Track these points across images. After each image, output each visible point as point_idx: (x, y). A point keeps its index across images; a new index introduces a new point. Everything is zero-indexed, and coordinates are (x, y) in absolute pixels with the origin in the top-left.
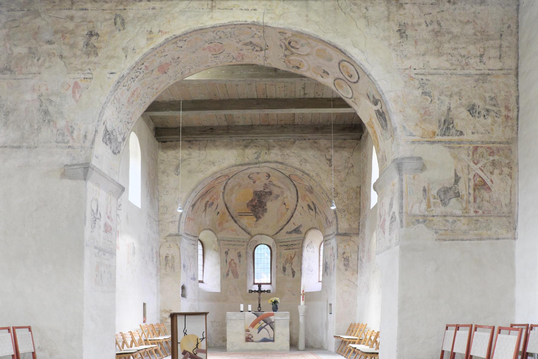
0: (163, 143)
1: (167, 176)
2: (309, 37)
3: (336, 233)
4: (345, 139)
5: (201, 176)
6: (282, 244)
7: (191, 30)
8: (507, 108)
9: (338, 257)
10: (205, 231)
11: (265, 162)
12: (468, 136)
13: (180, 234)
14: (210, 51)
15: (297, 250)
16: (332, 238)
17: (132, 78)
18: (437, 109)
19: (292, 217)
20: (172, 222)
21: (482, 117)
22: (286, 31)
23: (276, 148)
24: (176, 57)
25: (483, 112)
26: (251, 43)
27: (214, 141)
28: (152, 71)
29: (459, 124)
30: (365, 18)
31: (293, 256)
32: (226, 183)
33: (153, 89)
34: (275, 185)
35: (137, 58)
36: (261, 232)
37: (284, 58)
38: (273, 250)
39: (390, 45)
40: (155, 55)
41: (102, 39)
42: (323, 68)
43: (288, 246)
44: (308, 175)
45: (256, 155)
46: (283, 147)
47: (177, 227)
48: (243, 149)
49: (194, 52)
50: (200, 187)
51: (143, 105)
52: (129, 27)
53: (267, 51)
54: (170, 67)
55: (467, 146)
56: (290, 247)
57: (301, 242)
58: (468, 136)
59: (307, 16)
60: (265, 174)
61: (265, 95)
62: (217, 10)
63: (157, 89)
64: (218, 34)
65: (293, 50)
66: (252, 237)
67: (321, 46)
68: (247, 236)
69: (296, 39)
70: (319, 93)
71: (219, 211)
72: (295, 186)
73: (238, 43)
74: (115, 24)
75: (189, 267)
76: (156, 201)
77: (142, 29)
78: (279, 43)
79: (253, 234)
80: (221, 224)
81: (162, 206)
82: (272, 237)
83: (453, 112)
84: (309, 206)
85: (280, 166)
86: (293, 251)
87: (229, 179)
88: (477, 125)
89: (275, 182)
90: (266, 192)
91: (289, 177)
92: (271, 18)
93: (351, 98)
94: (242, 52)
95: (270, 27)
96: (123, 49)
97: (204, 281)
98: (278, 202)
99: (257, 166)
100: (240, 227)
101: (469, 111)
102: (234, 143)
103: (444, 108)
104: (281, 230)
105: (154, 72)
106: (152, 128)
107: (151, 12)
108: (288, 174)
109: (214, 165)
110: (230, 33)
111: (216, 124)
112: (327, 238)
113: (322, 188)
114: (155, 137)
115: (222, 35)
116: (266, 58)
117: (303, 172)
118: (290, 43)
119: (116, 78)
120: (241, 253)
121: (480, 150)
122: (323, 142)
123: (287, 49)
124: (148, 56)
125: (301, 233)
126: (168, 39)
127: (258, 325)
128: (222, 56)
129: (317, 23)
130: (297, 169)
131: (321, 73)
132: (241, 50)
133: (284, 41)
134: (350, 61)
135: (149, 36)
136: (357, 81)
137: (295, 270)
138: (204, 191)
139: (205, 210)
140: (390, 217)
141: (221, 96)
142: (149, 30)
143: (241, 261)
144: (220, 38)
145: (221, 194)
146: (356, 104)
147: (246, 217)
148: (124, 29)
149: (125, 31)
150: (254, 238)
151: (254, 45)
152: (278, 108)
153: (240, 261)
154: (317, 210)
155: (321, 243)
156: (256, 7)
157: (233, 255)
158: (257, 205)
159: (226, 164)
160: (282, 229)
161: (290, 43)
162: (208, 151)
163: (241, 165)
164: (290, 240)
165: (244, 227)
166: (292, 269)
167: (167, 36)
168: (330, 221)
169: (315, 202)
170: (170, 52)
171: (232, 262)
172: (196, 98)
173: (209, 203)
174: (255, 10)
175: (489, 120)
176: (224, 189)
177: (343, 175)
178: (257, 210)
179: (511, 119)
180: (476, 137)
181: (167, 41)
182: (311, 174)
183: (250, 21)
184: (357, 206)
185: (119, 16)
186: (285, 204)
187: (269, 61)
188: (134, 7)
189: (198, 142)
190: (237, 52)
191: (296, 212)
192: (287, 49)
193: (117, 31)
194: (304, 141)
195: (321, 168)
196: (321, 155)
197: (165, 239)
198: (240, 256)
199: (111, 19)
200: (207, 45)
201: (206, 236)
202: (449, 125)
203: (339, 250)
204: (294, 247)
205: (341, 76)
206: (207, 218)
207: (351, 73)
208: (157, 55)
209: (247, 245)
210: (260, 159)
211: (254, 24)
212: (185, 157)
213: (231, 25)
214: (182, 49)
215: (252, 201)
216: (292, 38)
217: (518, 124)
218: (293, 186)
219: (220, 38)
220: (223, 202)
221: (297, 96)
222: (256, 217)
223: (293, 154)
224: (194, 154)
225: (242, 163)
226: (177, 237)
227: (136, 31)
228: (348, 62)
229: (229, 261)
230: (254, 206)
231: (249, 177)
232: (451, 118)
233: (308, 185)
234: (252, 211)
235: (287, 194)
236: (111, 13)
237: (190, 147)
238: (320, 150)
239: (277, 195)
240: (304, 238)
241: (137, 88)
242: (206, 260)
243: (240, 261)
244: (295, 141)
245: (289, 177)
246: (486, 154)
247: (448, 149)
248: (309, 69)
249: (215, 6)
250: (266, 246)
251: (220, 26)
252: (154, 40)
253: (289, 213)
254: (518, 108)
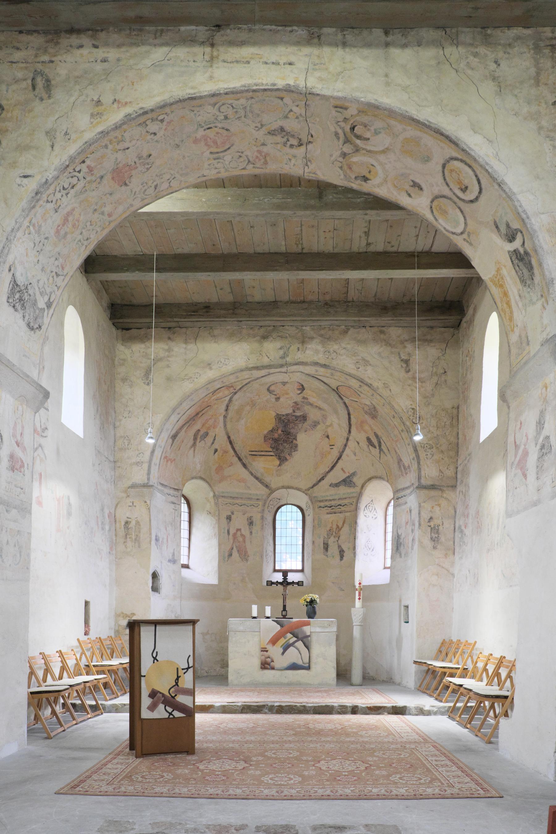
0: (124, 331)
1: (131, 386)
2: (391, 113)
3: (417, 484)
4: (432, 328)
5: (188, 387)
6: (322, 504)
7: (172, 100)
9: (420, 525)
10: (194, 481)
11: (296, 364)
13: (151, 483)
14: (206, 144)
15: (348, 514)
16: (410, 494)
17: (64, 188)
19: (339, 459)
20: (137, 463)
22: (347, 104)
23: (315, 341)
24: (145, 154)
26: (282, 129)
27: (211, 328)
28: (102, 177)
30: (494, 79)
31: (340, 525)
32: (230, 400)
33: (103, 213)
34: (311, 405)
35: (73, 149)
36: (286, 484)
37: (341, 159)
38: (306, 514)
39: (540, 128)
40: (106, 146)
41: (9, 115)
42: (412, 177)
43: (333, 508)
44: (369, 386)
45: (281, 352)
46: (329, 339)
47: (146, 472)
48: (260, 342)
49: (178, 146)
50: (186, 405)
51: (86, 243)
52: (59, 94)
53: (310, 147)
54: (133, 172)
56: (337, 510)
57: (355, 500)
59: (386, 76)
60: (296, 386)
61: (300, 246)
62: (221, 64)
63: (110, 215)
64: (223, 109)
65: (358, 142)
66: (272, 491)
67: (411, 132)
68: (264, 491)
69: (365, 119)
70: (393, 243)
71: (217, 447)
72: (347, 407)
73: (258, 129)
74: (34, 87)
75: (165, 541)
76: (111, 427)
77: (83, 97)
78: (333, 130)
79: (273, 486)
80: (220, 469)
81: (121, 437)
82: (305, 492)
84: (369, 439)
85: (322, 370)
86: (342, 516)
87: (235, 393)
89: (312, 400)
90: (296, 417)
91: (336, 391)
92: (321, 79)
93: (462, 233)
94: (265, 149)
95: (318, 95)
96: (47, 133)
97: (190, 565)
98: (317, 434)
99: (284, 369)
100: (252, 474)
102: (244, 331)
104: (320, 481)
105: (105, 181)
106: (105, 305)
107: (99, 67)
108: (334, 384)
109: (211, 369)
110: (245, 108)
111: (215, 299)
112: (399, 495)
113: (393, 408)
114: (110, 319)
115: (230, 112)
116: (307, 161)
117: (362, 381)
118: (353, 129)
119: (32, 185)
120: (254, 519)
122: (395, 332)
123: (347, 141)
124: (92, 147)
125: (354, 485)
126: (130, 115)
127: (282, 641)
128: (228, 157)
129: (405, 89)
130: (350, 375)
131: (407, 187)
132: (263, 144)
133: (342, 124)
134: (467, 158)
135: (96, 110)
136: (477, 199)
137: (344, 547)
138: (192, 412)
139: (194, 445)
140: (538, 447)
141: (224, 247)
142: (95, 99)
143: (254, 532)
144: (226, 118)
145: (221, 419)
146: (471, 244)
147: (263, 458)
148: (49, 97)
149: (51, 101)
150: (276, 494)
151: (288, 133)
152: (321, 268)
153: (251, 532)
154: (383, 447)
155: (389, 503)
156: (292, 59)
157: (239, 521)
158: (282, 439)
159: (230, 367)
160: (322, 479)
161: (353, 129)
162: (200, 345)
163: (257, 368)
164: (336, 497)
165: (259, 475)
166: (339, 547)
167: (128, 110)
168: (406, 464)
169: (379, 434)
170: (134, 142)
171: (239, 533)
172: (180, 251)
173: (201, 433)
174: (290, 64)
176: (227, 410)
177: (429, 386)
178: (281, 447)
181: (129, 119)
182: (375, 384)
183: (281, 83)
184: (452, 439)
185: (42, 74)
186: (328, 437)
187: (312, 167)
188: (69, 58)
189: (184, 330)
190: (255, 149)
191: (347, 451)
192: (347, 141)
193: (37, 100)
194: (364, 330)
195: (391, 375)
196: (392, 353)
197: (125, 492)
198: (251, 523)
199: (25, 80)
200: (201, 133)
201: (194, 488)
203: (422, 513)
204: (343, 508)
205: (446, 191)
206: (197, 459)
207: (466, 182)
208: (110, 147)
209: (264, 505)
210: (288, 359)
211: (288, 90)
212: (162, 354)
213: (247, 91)
214: (156, 138)
215: (272, 431)
216: (358, 118)
218: (342, 405)
219: (226, 118)
220: (224, 432)
221: (355, 249)
222: (279, 458)
223: (344, 351)
224: (176, 349)
225: (259, 365)
226: (145, 490)
227: (72, 100)
228: (462, 161)
229: (232, 531)
230: (276, 440)
231: (268, 390)
233: (368, 403)
234: (273, 448)
235: (332, 419)
236: (26, 68)
237: (169, 338)
238: (390, 345)
239: (315, 422)
240: (360, 495)
241: (73, 210)
242: (194, 530)
243: (251, 532)
244: (348, 329)
245: (336, 391)
248: (385, 181)
249: (217, 57)
250: (295, 508)
251: (226, 94)
252: (104, 117)
253: (335, 453)
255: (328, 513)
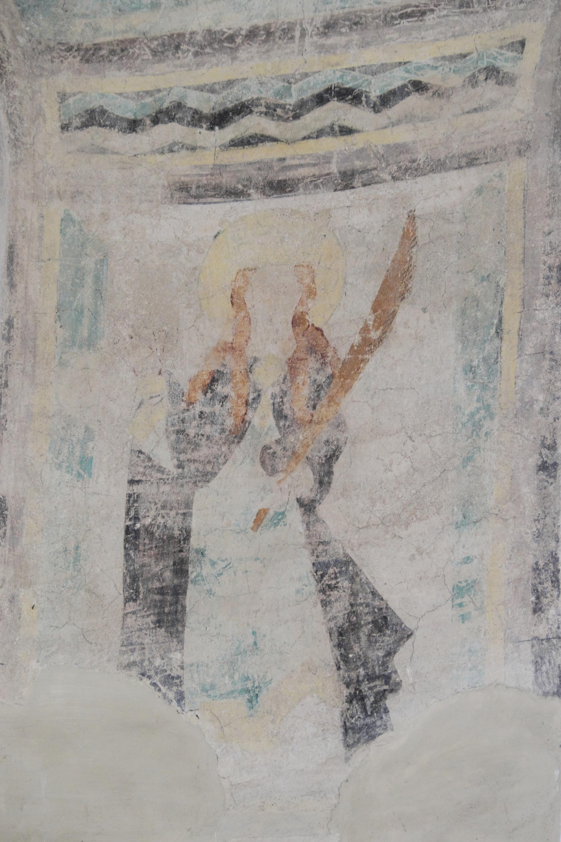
6: (116, 88)
31: (343, 317)
56: (297, 148)
137: (396, 577)
166: (332, 571)
255: (187, 192)
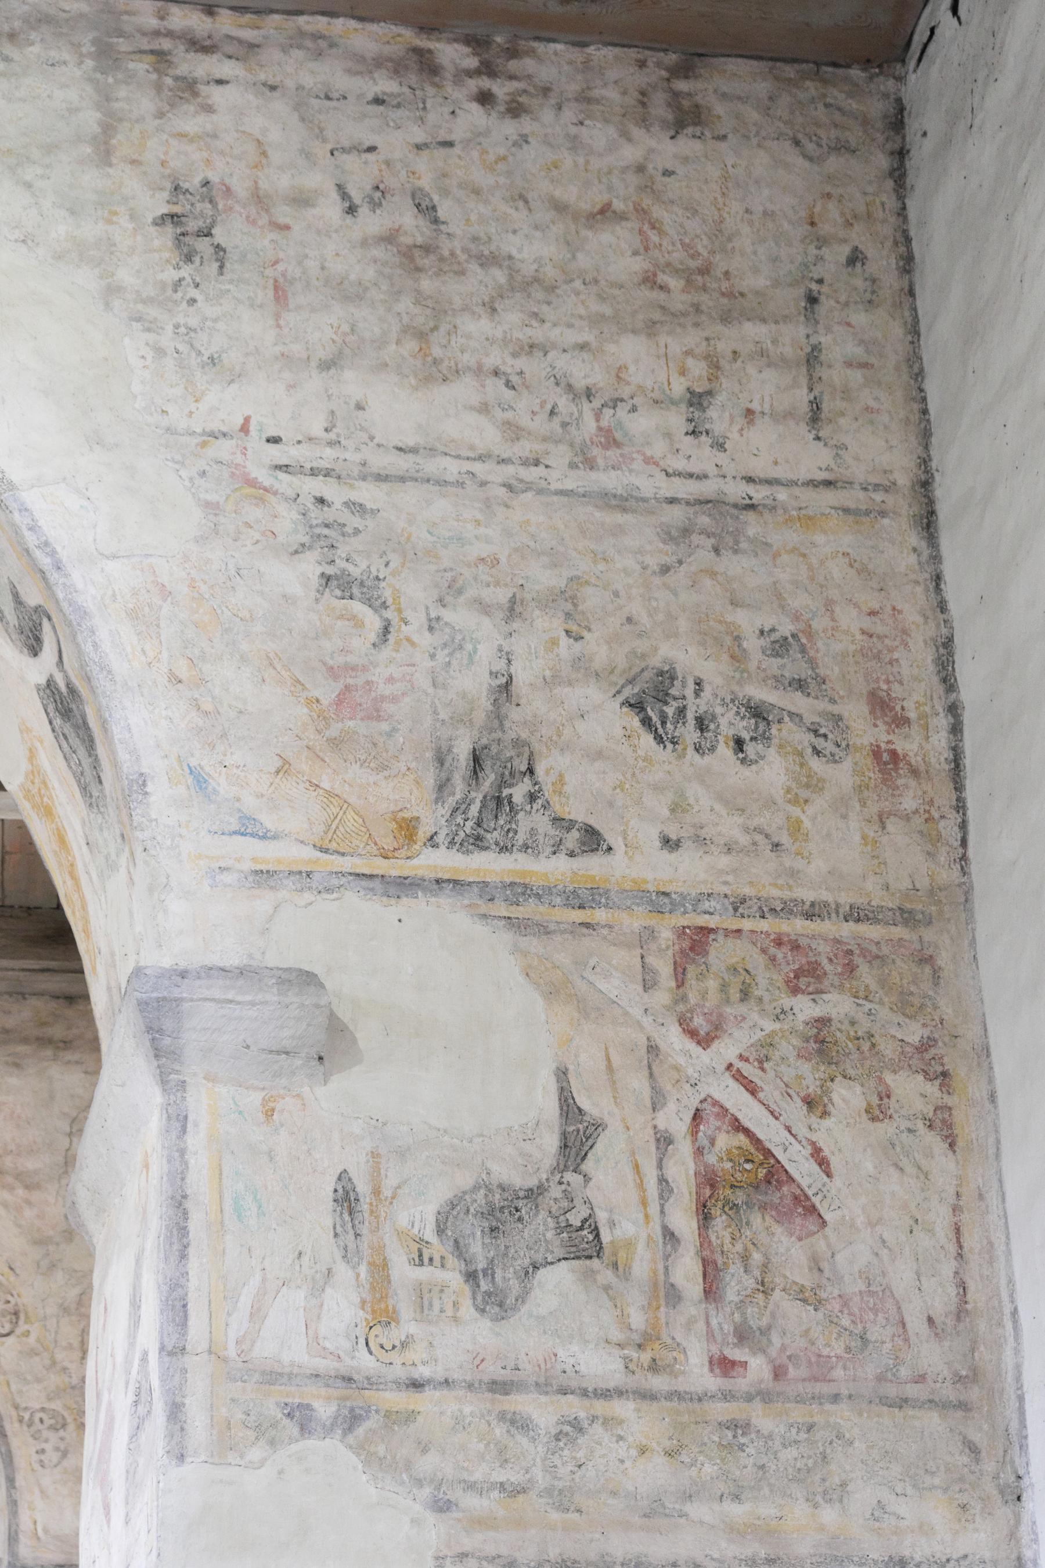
8: (881, 705)
12: (635, 861)
18: (423, 681)
21: (725, 751)
25: (731, 723)
29: (576, 783)
55: (634, 921)
58: (635, 861)
83: (532, 704)
88: (695, 791)
101: (637, 706)
103: (473, 682)
121: (722, 954)
175: (773, 772)
179: (915, 772)
180: (687, 871)
202: (502, 783)
217: (960, 806)
232: (518, 743)
246: (766, 980)
247: (507, 937)
254: (954, 710)
